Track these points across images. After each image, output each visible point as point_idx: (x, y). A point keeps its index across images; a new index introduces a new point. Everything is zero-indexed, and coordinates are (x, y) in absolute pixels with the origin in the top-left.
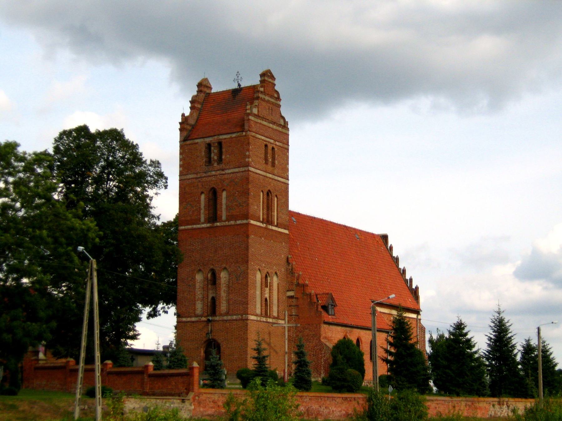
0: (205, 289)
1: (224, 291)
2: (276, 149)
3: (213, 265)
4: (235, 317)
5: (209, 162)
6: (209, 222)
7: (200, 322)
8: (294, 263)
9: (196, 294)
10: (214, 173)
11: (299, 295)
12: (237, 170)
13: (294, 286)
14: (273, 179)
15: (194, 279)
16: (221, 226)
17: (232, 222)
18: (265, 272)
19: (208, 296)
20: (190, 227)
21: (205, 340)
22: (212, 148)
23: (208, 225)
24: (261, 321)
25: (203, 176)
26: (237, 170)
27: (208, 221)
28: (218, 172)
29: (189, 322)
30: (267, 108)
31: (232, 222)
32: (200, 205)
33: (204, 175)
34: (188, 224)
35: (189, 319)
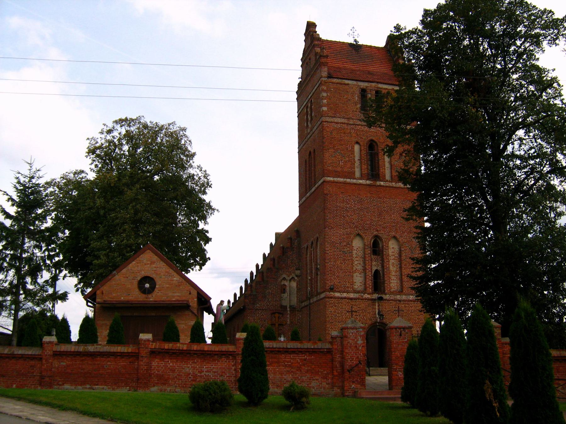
3: (377, 231)
7: (362, 299)
15: (349, 244)
20: (341, 180)
23: (368, 182)
25: (358, 123)
29: (345, 298)
32: (354, 157)
34: (339, 177)
35: (345, 295)
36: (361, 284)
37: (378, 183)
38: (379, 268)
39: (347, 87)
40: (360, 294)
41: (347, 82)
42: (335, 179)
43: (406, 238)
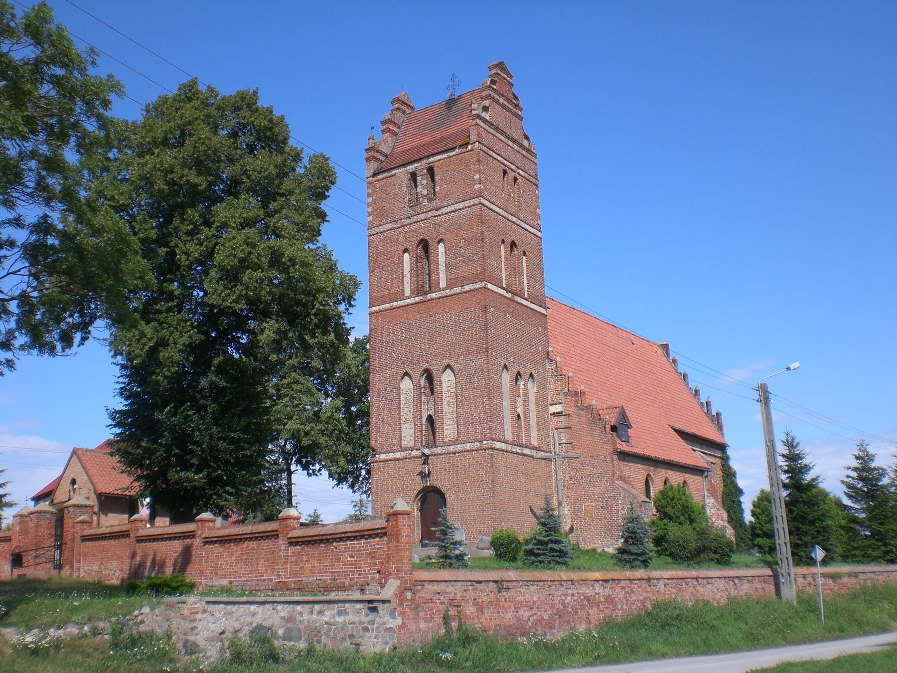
0: (418, 404)
1: (449, 402)
2: (520, 180)
5: (415, 201)
6: (418, 294)
7: (409, 458)
8: (558, 359)
9: (402, 414)
10: (422, 216)
11: (572, 410)
12: (461, 205)
13: (561, 396)
14: (518, 225)
16: (439, 298)
17: (457, 290)
18: (516, 371)
19: (421, 416)
21: (419, 488)
22: (419, 178)
23: (417, 299)
24: (512, 452)
25: (406, 223)
26: (461, 205)
27: (418, 291)
28: (430, 214)
29: (391, 460)
30: (503, 115)
31: (457, 290)
34: (385, 303)
35: (391, 456)
36: (411, 438)
37: (429, 296)
38: (432, 413)
39: (393, 179)
41: (393, 172)
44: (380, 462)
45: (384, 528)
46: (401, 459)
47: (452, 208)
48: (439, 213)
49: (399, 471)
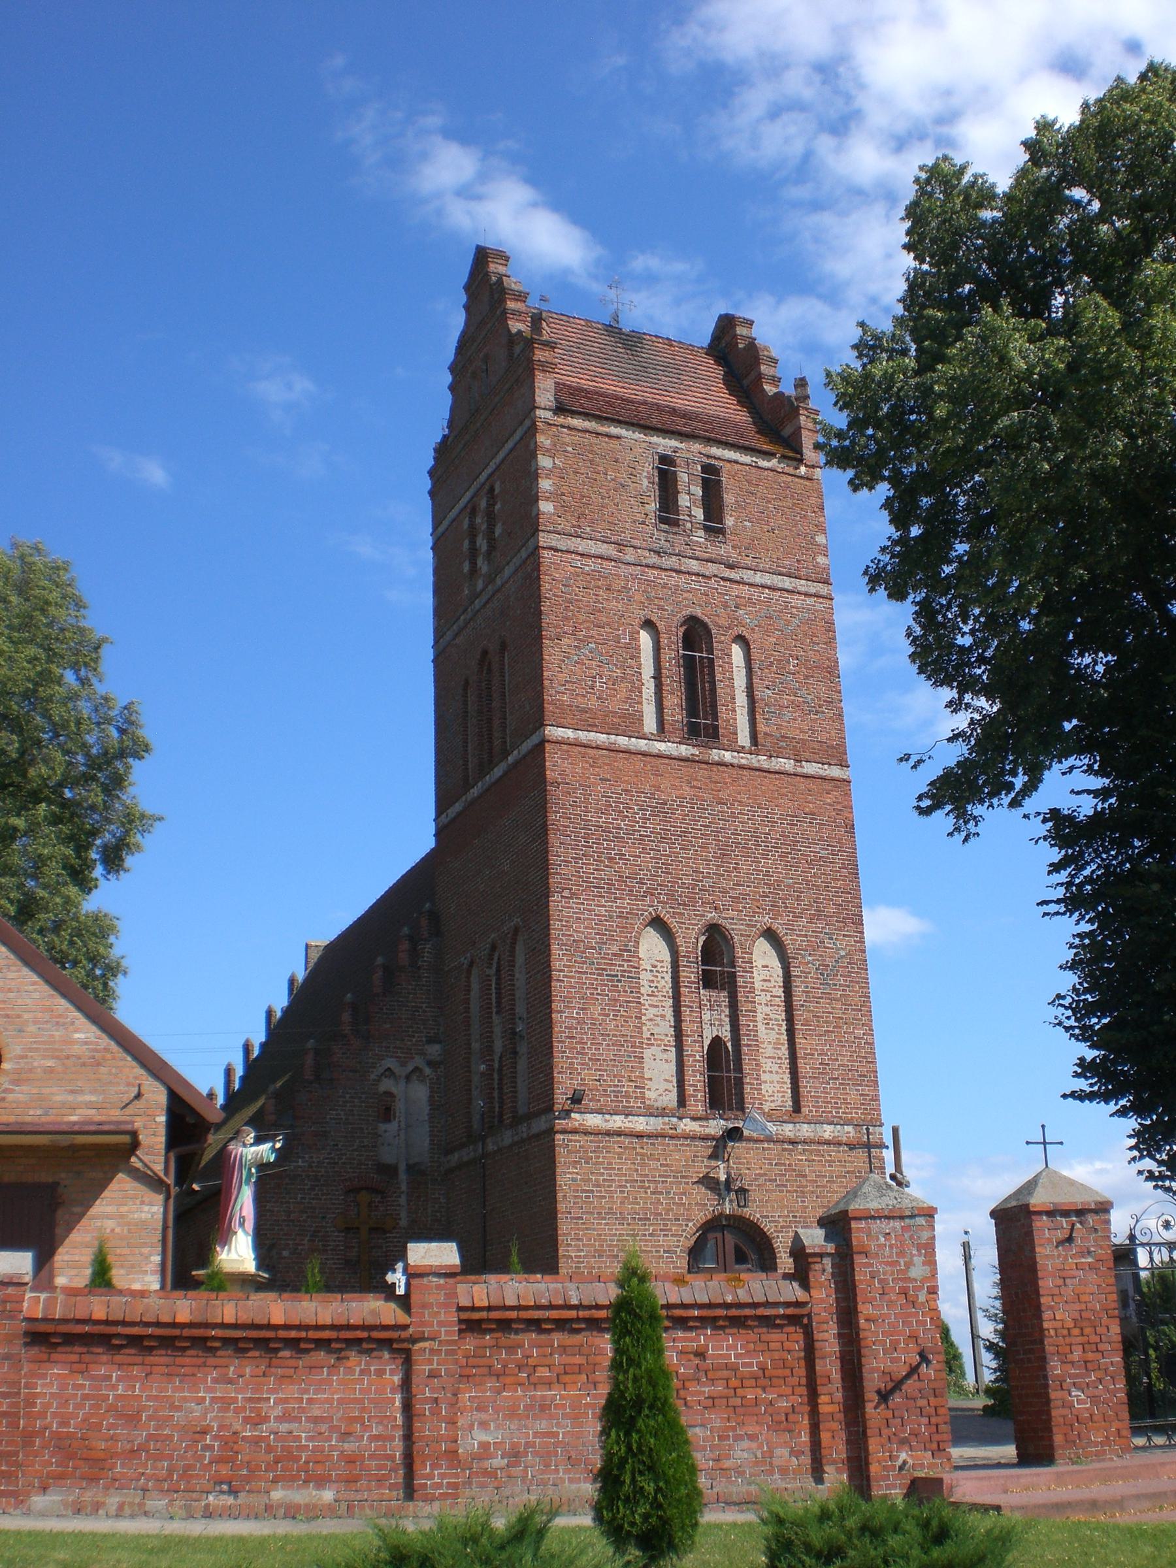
4: (828, 1131)
7: (672, 1137)
10: (694, 565)
15: (629, 952)
21: (701, 1216)
23: (684, 750)
25: (650, 561)
28: (711, 568)
29: (619, 1133)
32: (639, 667)
33: (653, 559)
35: (617, 1122)
37: (715, 755)
40: (667, 1119)
41: (614, 430)
42: (583, 736)
43: (806, 936)
44: (586, 1133)
45: (798, 1304)
46: (650, 1136)
47: (767, 579)
48: (733, 575)
49: (643, 1165)
